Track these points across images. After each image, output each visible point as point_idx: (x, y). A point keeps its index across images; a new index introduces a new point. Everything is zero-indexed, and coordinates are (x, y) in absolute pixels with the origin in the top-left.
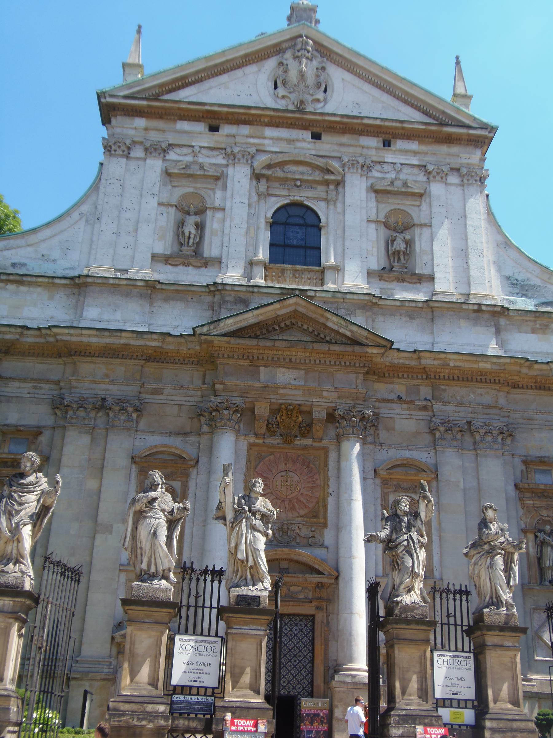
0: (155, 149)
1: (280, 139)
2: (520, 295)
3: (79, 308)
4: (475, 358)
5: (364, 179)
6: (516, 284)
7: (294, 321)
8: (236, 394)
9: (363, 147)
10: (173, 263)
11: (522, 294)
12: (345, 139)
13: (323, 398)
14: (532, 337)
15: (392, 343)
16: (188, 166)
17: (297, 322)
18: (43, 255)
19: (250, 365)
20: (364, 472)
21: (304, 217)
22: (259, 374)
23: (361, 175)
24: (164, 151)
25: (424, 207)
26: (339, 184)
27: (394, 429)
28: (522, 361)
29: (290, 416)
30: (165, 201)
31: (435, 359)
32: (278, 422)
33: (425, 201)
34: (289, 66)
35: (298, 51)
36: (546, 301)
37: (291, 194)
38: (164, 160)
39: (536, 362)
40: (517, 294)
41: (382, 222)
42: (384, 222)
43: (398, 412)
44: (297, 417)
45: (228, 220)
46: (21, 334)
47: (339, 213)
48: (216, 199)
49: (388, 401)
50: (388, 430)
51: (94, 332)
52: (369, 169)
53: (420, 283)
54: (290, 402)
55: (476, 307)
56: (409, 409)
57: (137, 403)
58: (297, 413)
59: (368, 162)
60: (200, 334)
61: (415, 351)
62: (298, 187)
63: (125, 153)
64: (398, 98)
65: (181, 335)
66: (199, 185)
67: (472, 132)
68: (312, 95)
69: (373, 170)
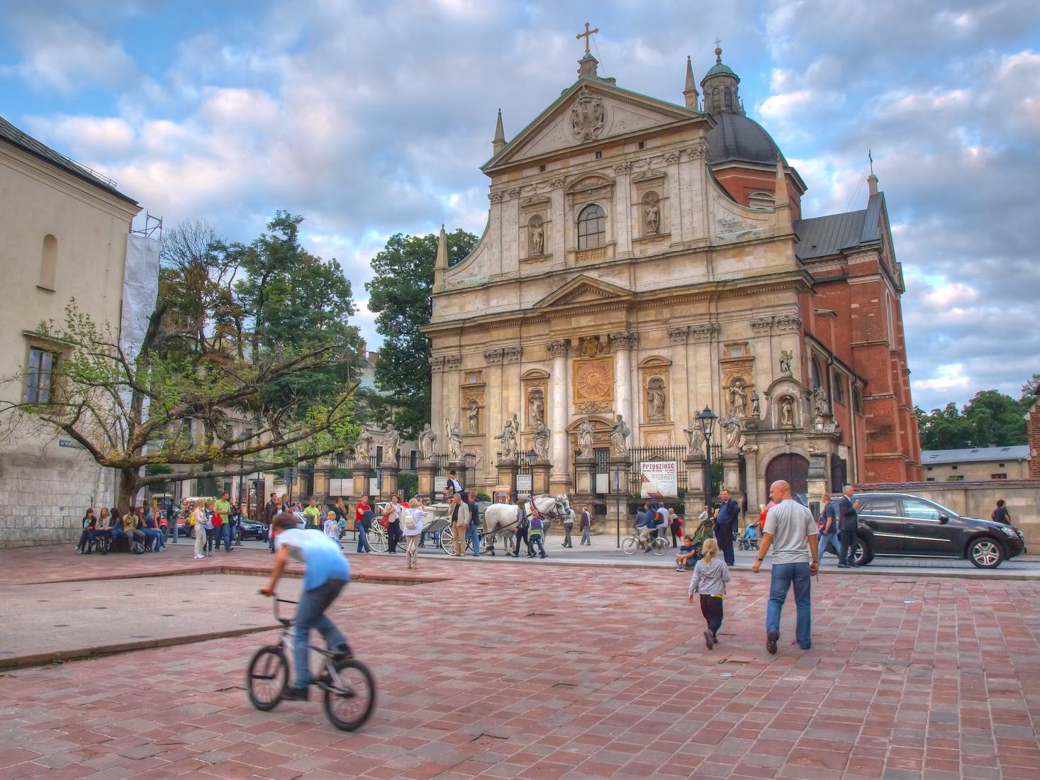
1: (579, 165)
3: (488, 301)
5: (628, 176)
9: (626, 154)
12: (615, 152)
14: (733, 261)
16: (531, 199)
20: (631, 367)
24: (519, 193)
25: (665, 186)
26: (613, 185)
50: (645, 339)
52: (631, 167)
57: (519, 349)
59: (629, 164)
64: (646, 109)
67: (691, 121)
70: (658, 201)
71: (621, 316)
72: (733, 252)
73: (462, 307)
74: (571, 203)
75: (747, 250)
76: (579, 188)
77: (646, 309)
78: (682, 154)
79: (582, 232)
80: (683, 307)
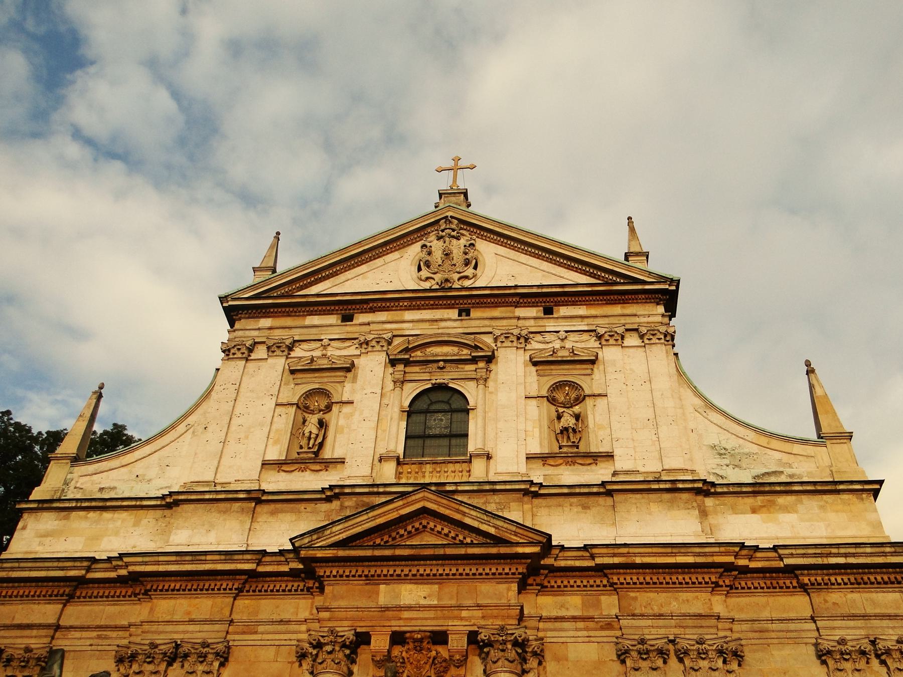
0: (279, 347)
2: (731, 467)
3: (166, 532)
4: (669, 550)
6: (725, 454)
7: (424, 522)
8: (346, 623)
9: (519, 318)
10: (288, 469)
11: (733, 465)
12: (497, 312)
13: (462, 619)
15: (550, 536)
17: (428, 523)
18: (137, 476)
19: (367, 584)
21: (451, 402)
22: (378, 593)
23: (517, 348)
24: (290, 348)
26: (490, 359)
27: (567, 660)
28: (737, 549)
29: (418, 648)
30: (285, 401)
31: (614, 555)
32: (403, 658)
33: (598, 368)
34: (433, 249)
35: (443, 231)
36: (767, 471)
37: (433, 378)
38: (287, 358)
39: (756, 548)
40: (727, 466)
41: (545, 397)
42: (547, 397)
43: (572, 633)
44: (430, 650)
45: (357, 413)
46: (89, 569)
47: (491, 393)
48: (344, 392)
49: (557, 619)
50: (558, 659)
51: (173, 558)
53: (596, 464)
54: (417, 628)
55: (668, 486)
56: (587, 629)
57: (221, 647)
58: (428, 643)
59: (524, 333)
60: (300, 547)
61: (586, 548)
62: (441, 368)
63: (244, 356)
64: (560, 265)
65: (282, 553)
66: (326, 380)
67: (647, 287)
68: (459, 273)
69: (532, 342)
70: (579, 400)
71: (508, 592)
72: (749, 501)
73: (96, 538)
74: (399, 376)
75: (782, 500)
76: (418, 355)
77: (558, 591)
78: (627, 335)
79: (418, 430)
80: (652, 595)
